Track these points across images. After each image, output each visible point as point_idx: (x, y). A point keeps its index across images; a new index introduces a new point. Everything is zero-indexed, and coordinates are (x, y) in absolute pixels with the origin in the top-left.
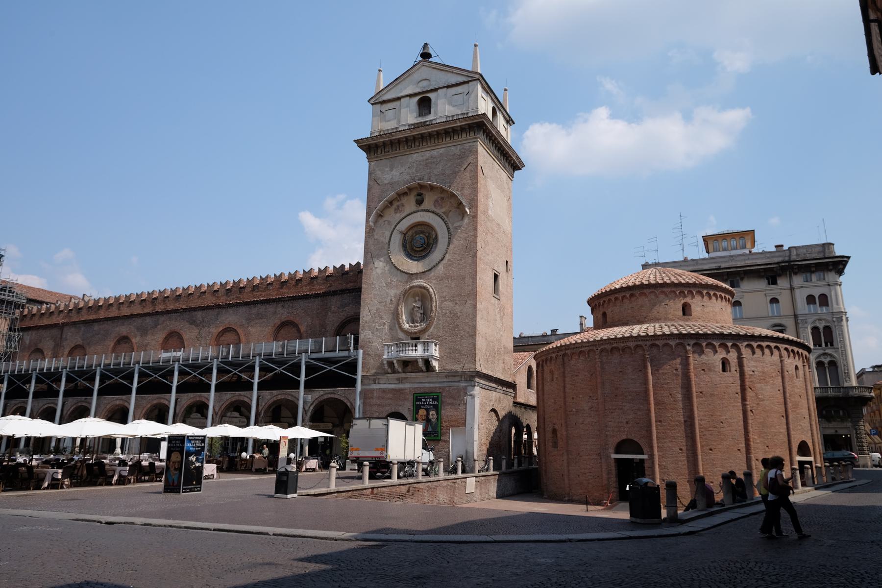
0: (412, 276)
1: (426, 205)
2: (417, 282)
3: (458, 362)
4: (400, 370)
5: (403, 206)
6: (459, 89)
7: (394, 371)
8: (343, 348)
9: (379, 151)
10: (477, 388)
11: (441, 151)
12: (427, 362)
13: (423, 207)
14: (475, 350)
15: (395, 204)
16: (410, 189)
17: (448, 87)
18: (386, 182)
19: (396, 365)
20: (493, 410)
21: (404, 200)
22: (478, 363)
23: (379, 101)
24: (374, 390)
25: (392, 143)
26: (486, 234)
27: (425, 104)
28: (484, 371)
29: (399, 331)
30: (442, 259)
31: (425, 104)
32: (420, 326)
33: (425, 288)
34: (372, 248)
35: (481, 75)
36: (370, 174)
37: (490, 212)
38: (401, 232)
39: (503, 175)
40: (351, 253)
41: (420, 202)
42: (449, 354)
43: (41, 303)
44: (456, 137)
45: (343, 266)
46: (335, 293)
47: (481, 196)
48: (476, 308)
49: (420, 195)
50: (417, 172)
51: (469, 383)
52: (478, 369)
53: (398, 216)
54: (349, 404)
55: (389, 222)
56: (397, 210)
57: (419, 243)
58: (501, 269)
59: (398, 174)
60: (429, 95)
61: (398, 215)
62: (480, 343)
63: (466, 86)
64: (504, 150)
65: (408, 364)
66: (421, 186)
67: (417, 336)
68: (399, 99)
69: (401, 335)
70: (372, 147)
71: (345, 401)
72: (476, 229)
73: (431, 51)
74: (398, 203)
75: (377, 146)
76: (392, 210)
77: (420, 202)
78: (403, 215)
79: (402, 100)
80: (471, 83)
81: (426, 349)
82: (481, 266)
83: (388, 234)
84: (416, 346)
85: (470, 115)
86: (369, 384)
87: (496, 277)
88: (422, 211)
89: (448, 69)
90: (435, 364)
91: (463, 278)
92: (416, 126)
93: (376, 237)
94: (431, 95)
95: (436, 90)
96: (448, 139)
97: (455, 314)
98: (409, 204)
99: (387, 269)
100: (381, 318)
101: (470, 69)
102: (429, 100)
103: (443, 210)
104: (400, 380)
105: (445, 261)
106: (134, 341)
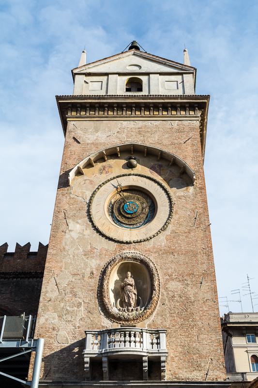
2: (130, 252)
3: (199, 367)
5: (110, 167)
8: (11, 335)
17: (161, 74)
18: (89, 142)
19: (105, 365)
21: (111, 162)
27: (135, 84)
30: (164, 228)
33: (142, 261)
34: (66, 207)
48: (216, 292)
50: (128, 137)
53: (104, 177)
55: (91, 182)
56: (101, 171)
68: (107, 74)
72: (205, 201)
74: (104, 164)
83: (89, 194)
88: (133, 175)
91: (195, 255)
93: (72, 196)
94: (144, 79)
97: (187, 299)
100: (75, 296)
105: (168, 232)
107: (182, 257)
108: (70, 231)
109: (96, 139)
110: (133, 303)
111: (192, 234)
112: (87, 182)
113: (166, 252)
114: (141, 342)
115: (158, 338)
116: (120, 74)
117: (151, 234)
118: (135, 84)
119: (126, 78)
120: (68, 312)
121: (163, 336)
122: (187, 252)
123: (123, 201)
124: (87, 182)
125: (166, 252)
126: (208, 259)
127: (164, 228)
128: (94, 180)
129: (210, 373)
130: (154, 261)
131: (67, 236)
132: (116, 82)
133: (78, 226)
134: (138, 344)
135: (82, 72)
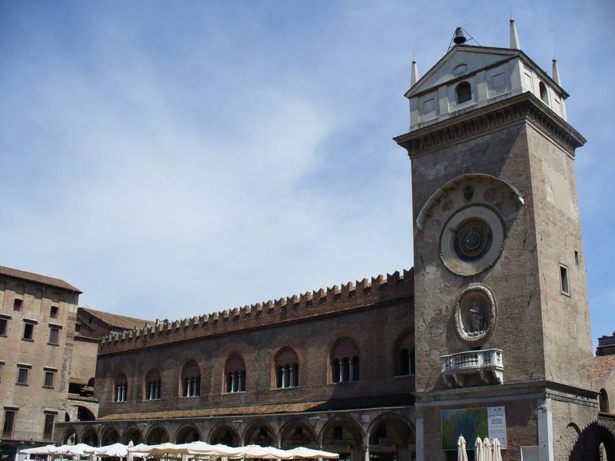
0: (468, 279)
4: (461, 384)
5: (451, 202)
6: (498, 70)
7: (455, 386)
9: (421, 146)
10: (548, 401)
11: (487, 138)
12: (489, 372)
14: (543, 356)
15: (443, 202)
16: (457, 183)
17: (487, 69)
18: (431, 178)
19: (456, 379)
20: (572, 425)
22: (547, 372)
23: (418, 94)
24: (434, 407)
25: (433, 136)
26: (547, 224)
28: (557, 381)
29: (457, 340)
30: (499, 257)
31: (464, 91)
32: (480, 335)
35: (521, 52)
36: (414, 171)
37: (549, 199)
38: (452, 230)
39: (562, 155)
40: (403, 261)
42: (515, 363)
43: (121, 330)
44: (501, 121)
45: (397, 273)
46: (391, 303)
47: (534, 183)
48: (540, 309)
49: (468, 188)
51: (539, 395)
52: (549, 378)
54: (409, 424)
55: (438, 222)
56: (446, 207)
57: (473, 243)
58: (569, 261)
59: (443, 168)
60: (467, 80)
61: (447, 212)
62: (549, 348)
63: (506, 65)
64: (559, 127)
65: (471, 378)
66: (469, 179)
68: (436, 88)
70: (410, 142)
72: (533, 220)
73: (465, 35)
75: (418, 141)
76: (440, 208)
77: (469, 195)
78: (452, 212)
79: (440, 89)
80: (510, 62)
81: (487, 357)
82: (542, 261)
83: (438, 234)
84: (476, 357)
85: (513, 95)
86: (429, 401)
87: (563, 271)
89: (484, 50)
90: (499, 375)
92: (455, 116)
93: (425, 240)
94: (470, 80)
95: (473, 74)
96: (493, 124)
98: (458, 200)
99: (439, 273)
101: (509, 47)
102: (468, 85)
103: (495, 202)
104: (462, 396)
105: (502, 259)
106: (200, 364)
108: (427, 273)
109: (437, 173)
110: (478, 326)
111: (522, 257)
112: (435, 222)
114: (476, 361)
119: (454, 86)
124: (435, 222)
126: (535, 280)
129: (534, 375)
131: (426, 279)
134: (474, 363)
135: (415, 94)
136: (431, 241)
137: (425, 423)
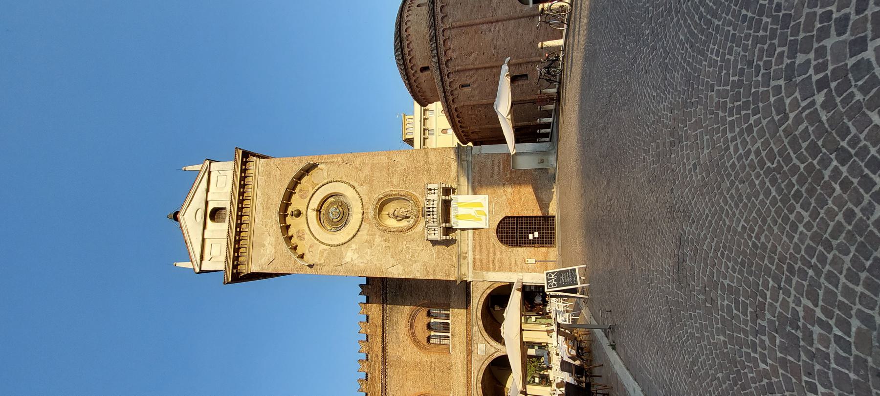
1: (303, 209)
2: (371, 213)
3: (449, 164)
5: (298, 231)
11: (259, 194)
13: (303, 211)
17: (208, 191)
30: (354, 187)
41: (299, 214)
46: (384, 350)
53: (308, 236)
54: (488, 291)
56: (301, 238)
59: (269, 239)
61: (306, 237)
67: (421, 209)
68: (203, 240)
69: (420, 226)
71: (485, 296)
77: (299, 214)
78: (307, 230)
93: (322, 261)
95: (207, 202)
103: (310, 189)
105: (356, 185)
107: (375, 174)
113: (371, 186)
115: (430, 190)
116: (204, 228)
117: (358, 197)
118: (216, 214)
120: (413, 256)
121: (429, 186)
122: (371, 170)
123: (331, 222)
125: (371, 186)
127: (354, 187)
128: (309, 244)
130: (378, 195)
131: (356, 262)
132: (213, 231)
133: (348, 254)
136: (325, 254)
137: (487, 270)
